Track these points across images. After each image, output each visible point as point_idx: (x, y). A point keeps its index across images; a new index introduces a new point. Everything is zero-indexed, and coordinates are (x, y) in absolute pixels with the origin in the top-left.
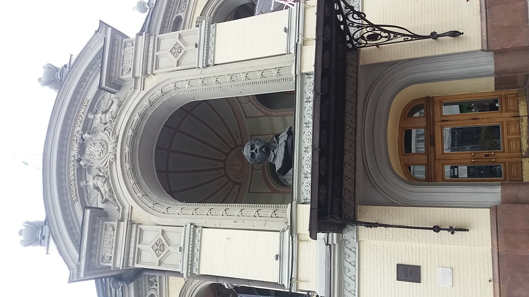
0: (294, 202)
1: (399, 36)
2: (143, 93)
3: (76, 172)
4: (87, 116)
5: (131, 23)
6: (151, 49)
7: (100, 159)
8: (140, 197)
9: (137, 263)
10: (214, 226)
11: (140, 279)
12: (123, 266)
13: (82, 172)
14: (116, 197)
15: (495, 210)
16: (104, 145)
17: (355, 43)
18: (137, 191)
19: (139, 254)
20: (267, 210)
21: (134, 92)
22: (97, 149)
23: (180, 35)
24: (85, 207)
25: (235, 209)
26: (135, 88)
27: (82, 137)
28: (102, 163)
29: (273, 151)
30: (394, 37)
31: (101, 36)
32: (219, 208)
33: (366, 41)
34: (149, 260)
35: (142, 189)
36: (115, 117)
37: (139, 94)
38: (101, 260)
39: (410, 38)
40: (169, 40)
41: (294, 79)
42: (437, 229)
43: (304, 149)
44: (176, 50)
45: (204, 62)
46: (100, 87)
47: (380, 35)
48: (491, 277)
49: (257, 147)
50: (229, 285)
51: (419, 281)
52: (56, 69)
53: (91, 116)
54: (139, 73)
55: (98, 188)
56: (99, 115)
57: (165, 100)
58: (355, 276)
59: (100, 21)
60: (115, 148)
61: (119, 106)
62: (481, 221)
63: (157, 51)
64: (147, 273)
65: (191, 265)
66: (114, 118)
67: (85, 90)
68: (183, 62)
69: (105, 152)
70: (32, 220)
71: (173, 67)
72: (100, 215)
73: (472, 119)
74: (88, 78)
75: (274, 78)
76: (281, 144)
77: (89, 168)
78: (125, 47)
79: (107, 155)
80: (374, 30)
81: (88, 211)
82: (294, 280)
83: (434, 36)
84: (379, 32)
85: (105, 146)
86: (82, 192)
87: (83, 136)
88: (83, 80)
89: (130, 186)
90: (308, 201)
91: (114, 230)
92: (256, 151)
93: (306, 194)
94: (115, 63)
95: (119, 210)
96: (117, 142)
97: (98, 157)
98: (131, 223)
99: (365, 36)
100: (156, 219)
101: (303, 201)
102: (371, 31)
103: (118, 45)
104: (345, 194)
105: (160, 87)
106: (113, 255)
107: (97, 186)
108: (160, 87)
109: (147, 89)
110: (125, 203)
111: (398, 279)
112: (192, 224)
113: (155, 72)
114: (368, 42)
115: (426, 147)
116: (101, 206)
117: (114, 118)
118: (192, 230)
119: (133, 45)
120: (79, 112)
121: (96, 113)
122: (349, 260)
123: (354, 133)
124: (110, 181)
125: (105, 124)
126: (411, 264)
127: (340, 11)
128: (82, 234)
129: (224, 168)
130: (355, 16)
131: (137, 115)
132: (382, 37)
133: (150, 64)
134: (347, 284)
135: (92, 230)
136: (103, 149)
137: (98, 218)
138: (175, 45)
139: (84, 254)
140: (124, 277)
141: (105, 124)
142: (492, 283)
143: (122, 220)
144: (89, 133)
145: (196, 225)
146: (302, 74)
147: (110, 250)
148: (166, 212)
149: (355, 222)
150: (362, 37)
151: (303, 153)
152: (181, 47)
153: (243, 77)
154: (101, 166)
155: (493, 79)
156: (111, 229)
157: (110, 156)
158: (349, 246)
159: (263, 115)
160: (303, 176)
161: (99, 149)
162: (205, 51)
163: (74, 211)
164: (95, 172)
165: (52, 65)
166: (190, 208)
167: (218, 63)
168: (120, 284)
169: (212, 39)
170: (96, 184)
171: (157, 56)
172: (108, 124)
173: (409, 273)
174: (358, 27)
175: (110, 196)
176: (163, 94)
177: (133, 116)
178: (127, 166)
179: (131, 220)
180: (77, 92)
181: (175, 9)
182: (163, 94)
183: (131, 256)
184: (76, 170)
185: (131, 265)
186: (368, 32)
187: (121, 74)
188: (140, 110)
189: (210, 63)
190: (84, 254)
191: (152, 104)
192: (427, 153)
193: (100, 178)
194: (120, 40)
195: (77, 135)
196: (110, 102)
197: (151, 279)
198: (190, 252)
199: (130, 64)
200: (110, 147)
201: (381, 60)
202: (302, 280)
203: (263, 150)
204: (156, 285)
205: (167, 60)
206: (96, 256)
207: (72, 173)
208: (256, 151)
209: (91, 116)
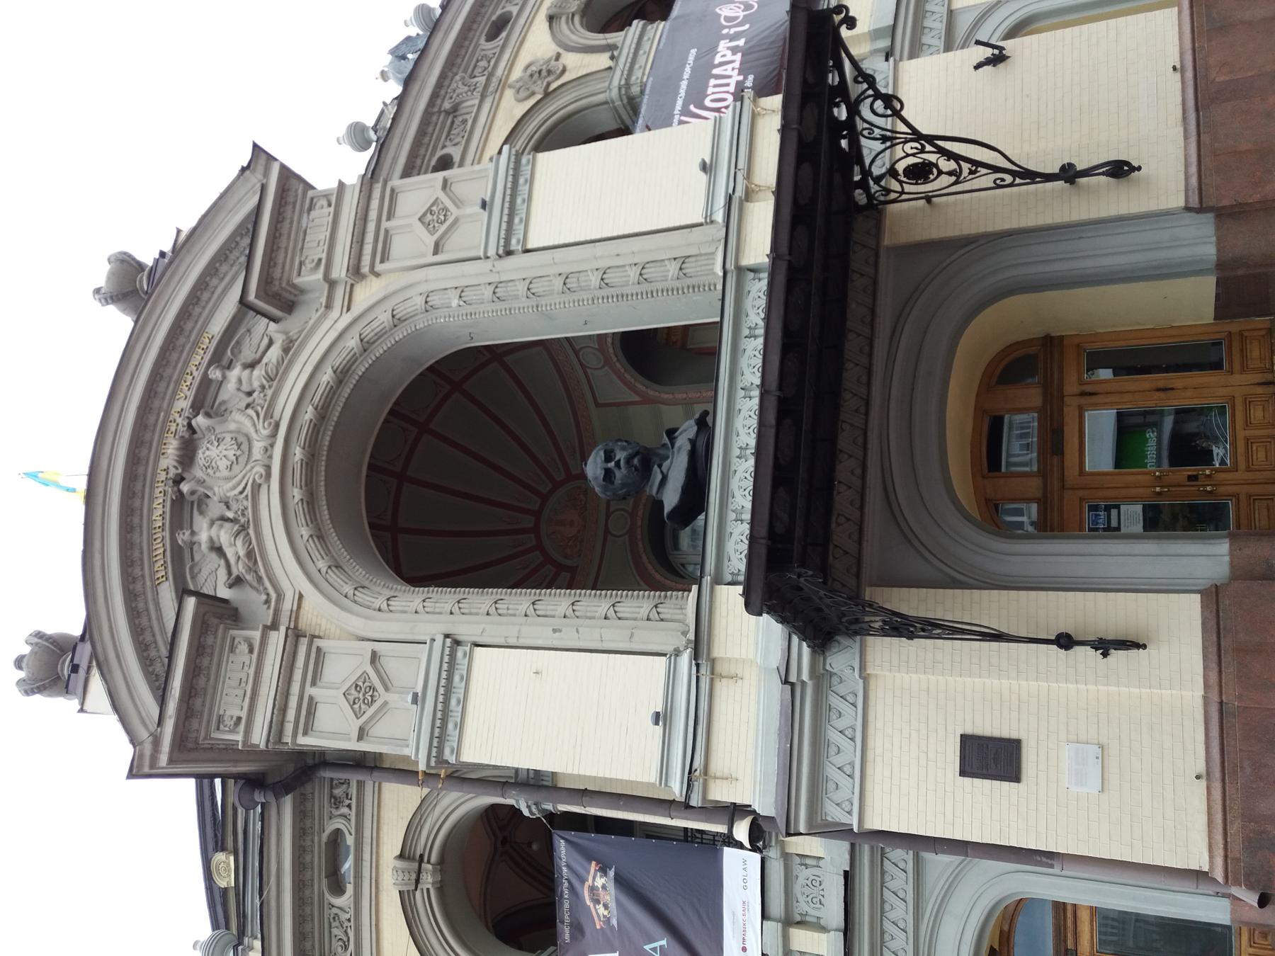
0: (707, 580)
1: (983, 171)
2: (347, 319)
3: (168, 509)
4: (206, 374)
5: (331, 165)
6: (373, 215)
7: (228, 479)
8: (324, 571)
9: (305, 734)
10: (501, 641)
11: (308, 787)
12: (268, 741)
13: (183, 508)
14: (262, 572)
15: (1213, 597)
16: (242, 443)
17: (874, 188)
18: (315, 554)
19: (311, 712)
20: (637, 604)
21: (324, 316)
22: (225, 453)
23: (445, 181)
24: (183, 592)
25: (557, 602)
26: (329, 306)
27: (190, 426)
28: (234, 488)
29: (660, 466)
30: (971, 172)
31: (255, 179)
32: (519, 600)
33: (901, 182)
34: (334, 729)
35: (328, 551)
36: (275, 378)
37: (337, 320)
38: (213, 726)
39: (1009, 179)
40: (419, 193)
41: (720, 287)
42: (1065, 641)
43: (737, 452)
44: (433, 217)
45: (502, 243)
46: (243, 301)
47: (936, 166)
48: (1201, 767)
49: (621, 455)
50: (534, 809)
51: (1017, 779)
52: (140, 267)
53: (215, 374)
54: (340, 270)
55: (219, 550)
57: (399, 335)
58: (852, 764)
59: (255, 146)
60: (268, 450)
61: (286, 350)
62: (1179, 625)
63: (388, 219)
64: (328, 774)
65: (439, 736)
66: (270, 379)
67: (207, 311)
69: (242, 460)
70: (50, 630)
71: (423, 256)
72: (219, 614)
73: (1158, 390)
74: (215, 281)
75: (670, 284)
76: (680, 448)
77: (202, 502)
78: (310, 209)
79: (248, 467)
80: (923, 151)
81: (191, 602)
82: (697, 773)
83: (1069, 174)
84: (933, 158)
85: (245, 447)
86: (181, 557)
87: (193, 422)
88: (202, 285)
89: (300, 545)
90: (752, 275)
91: (251, 651)
92: (618, 464)
93: (737, 560)
94: (283, 245)
95: (267, 602)
96: (274, 435)
97: (225, 473)
98: (296, 634)
99: (900, 167)
100: (357, 624)
101: (729, 578)
102: (913, 155)
103: (294, 204)
104: (838, 524)
105: (389, 305)
106: (244, 714)
107: (217, 545)
108: (389, 305)
109: (357, 309)
111: (963, 773)
112: (447, 636)
113: (379, 267)
114: (907, 188)
115: (1042, 459)
116: (224, 593)
118: (447, 651)
119: (330, 205)
120: (187, 363)
121: (229, 366)
122: (841, 724)
123: (863, 410)
124: (251, 531)
125: (250, 394)
126: (997, 734)
127: (842, 88)
128: (171, 657)
129: (536, 530)
130: (879, 105)
131: (330, 371)
132: (940, 173)
133: (368, 249)
134: (831, 786)
135: (198, 649)
136: (238, 453)
137: (216, 621)
138: (433, 205)
140: (270, 780)
141: (250, 394)
142: (1203, 783)
143: (274, 626)
144: (208, 415)
145: (459, 638)
146: (740, 270)
147: (238, 701)
148: (384, 606)
149: (857, 629)
150: (892, 172)
151: (734, 460)
152: (446, 209)
153: (594, 279)
154: (232, 494)
155: (1211, 281)
156: (244, 647)
157: (255, 470)
158: (842, 689)
159: (637, 399)
160: (732, 516)
161: (230, 454)
162: (505, 218)
163: (157, 604)
164: (215, 509)
165: (130, 256)
166: (444, 598)
167: (535, 246)
168: (259, 797)
169: (523, 189)
170: (215, 539)
171: (387, 231)
172: (255, 395)
173: (991, 758)
174: (884, 139)
175: (249, 570)
176: (397, 321)
177: (318, 375)
178: (296, 494)
179: (296, 627)
180: (185, 314)
181: (438, 139)
182: (397, 321)
183: (291, 715)
184: (168, 504)
185: (288, 738)
186: (908, 155)
187: (295, 272)
188: (337, 359)
189: (514, 245)
191: (366, 345)
192: (1043, 473)
193: (227, 525)
194: (300, 191)
195: (179, 420)
196: (266, 341)
197: (337, 792)
198: (440, 707)
199: (320, 249)
200: (258, 447)
201: (936, 234)
202: (718, 774)
203: (636, 461)
204: (349, 806)
205: (410, 241)
206: (202, 715)
207: (159, 510)
208: (618, 464)
209: (215, 374)
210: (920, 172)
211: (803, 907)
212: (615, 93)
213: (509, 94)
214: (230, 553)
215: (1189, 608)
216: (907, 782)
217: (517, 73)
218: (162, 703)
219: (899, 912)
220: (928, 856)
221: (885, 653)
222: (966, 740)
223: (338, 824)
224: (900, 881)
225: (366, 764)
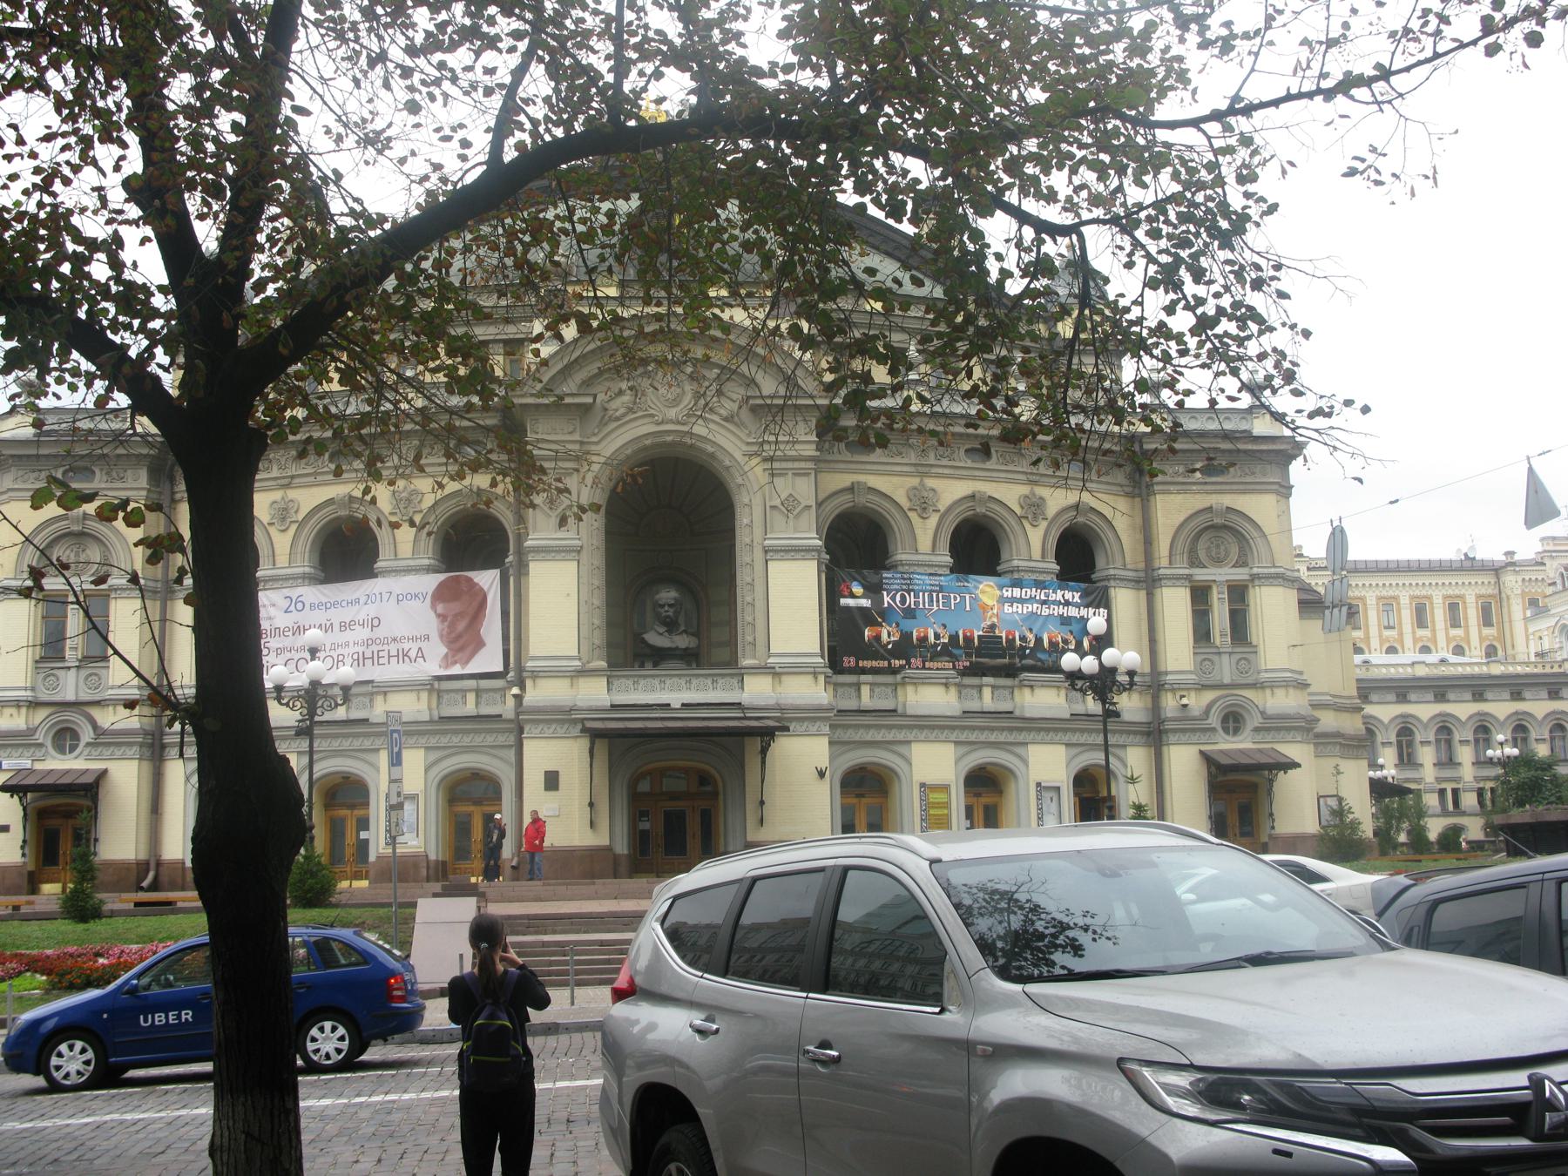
6: (797, 465)
15: (609, 849)
20: (599, 638)
25: (598, 600)
32: (599, 580)
42: (591, 805)
68: (775, 512)
81: (589, 400)
83: (762, 803)
96: (679, 423)
110: (604, 443)
139: (541, 401)
190: (541, 401)
196: (735, 396)
200: (672, 413)
212: (899, 557)
213: (915, 481)
216: (541, 753)
217: (931, 483)
219: (490, 739)
220: (513, 751)
221: (584, 743)
222: (556, 774)
224: (501, 739)
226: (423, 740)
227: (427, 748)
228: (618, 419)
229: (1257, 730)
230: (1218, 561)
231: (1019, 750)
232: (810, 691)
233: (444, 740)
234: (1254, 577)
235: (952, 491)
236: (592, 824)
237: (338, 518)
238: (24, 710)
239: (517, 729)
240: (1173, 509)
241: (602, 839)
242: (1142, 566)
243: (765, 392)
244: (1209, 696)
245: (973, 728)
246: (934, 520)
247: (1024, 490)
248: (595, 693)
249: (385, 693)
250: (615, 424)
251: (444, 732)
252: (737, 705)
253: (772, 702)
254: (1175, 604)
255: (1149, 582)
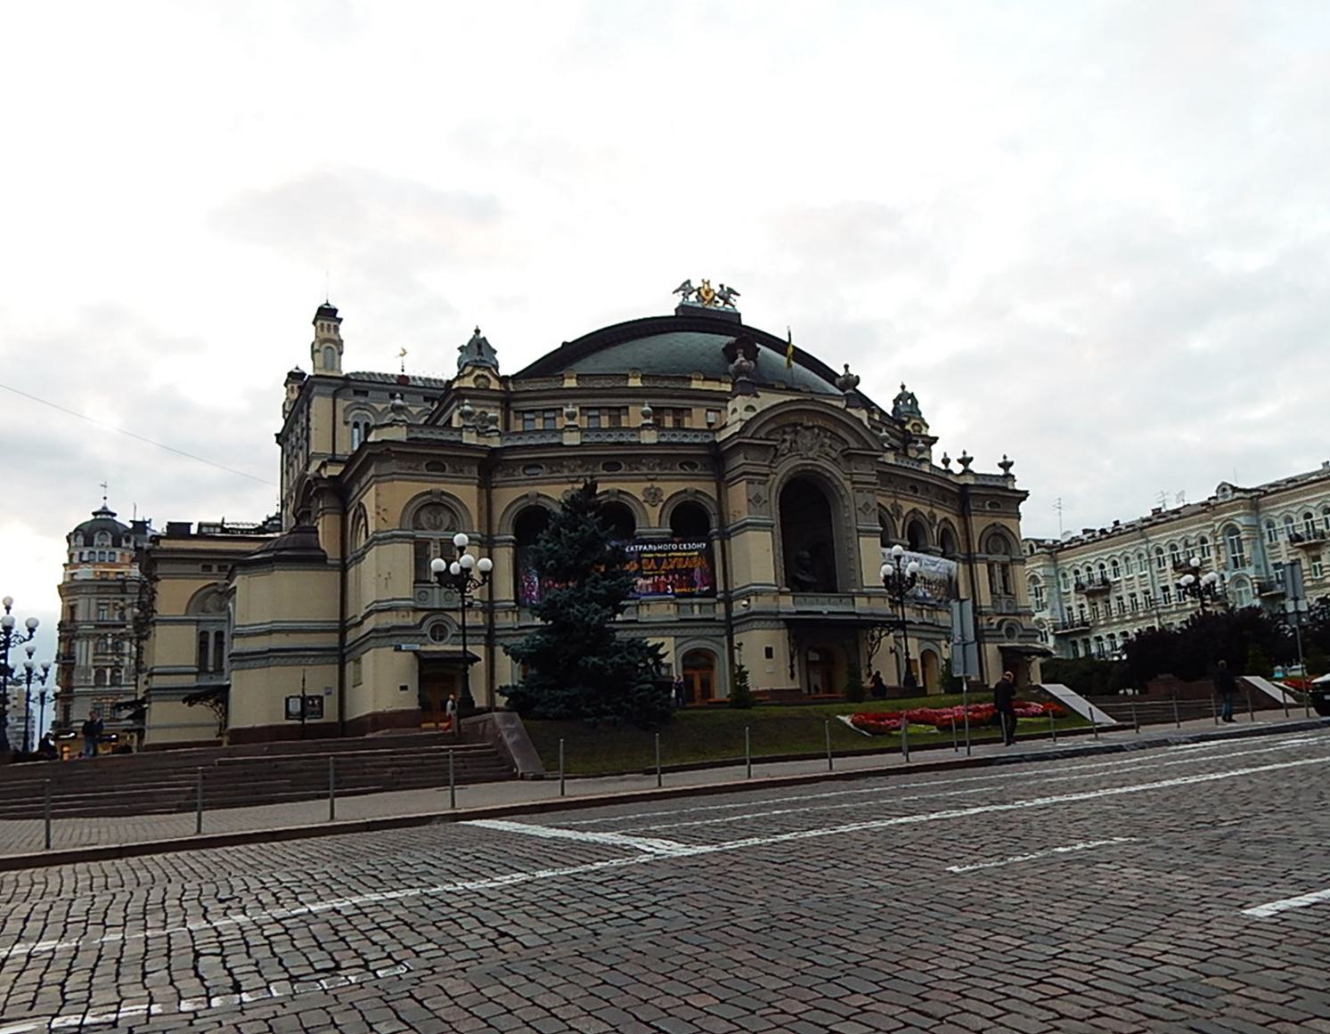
15: (800, 690)
54: (856, 478)
56: (826, 440)
57: (838, 496)
77: (796, 433)
98: (767, 475)
117: (827, 454)
176: (842, 496)
188: (834, 479)
191: (836, 486)
200: (811, 454)
205: (861, 499)
207: (793, 419)
210: (873, 638)
211: (704, 608)
213: (892, 500)
214: (783, 447)
215: (798, 687)
217: (899, 502)
218: (751, 438)
219: (711, 632)
220: (725, 638)
223: (700, 467)
224: (718, 632)
225: (722, 481)
226: (673, 632)
227: (676, 637)
228: (784, 455)
229: (1020, 636)
230: (997, 552)
231: (937, 643)
232: (882, 607)
233: (686, 632)
234: (1012, 560)
235: (907, 507)
236: (792, 676)
237: (610, 502)
238: (411, 613)
239: (730, 625)
240: (978, 524)
241: (795, 685)
242: (965, 551)
243: (851, 446)
244: (1000, 618)
245: (923, 631)
246: (902, 520)
247: (929, 509)
248: (787, 604)
249: (648, 605)
250: (783, 458)
251: (685, 628)
252: (853, 613)
253: (868, 611)
254: (982, 569)
255: (969, 560)
